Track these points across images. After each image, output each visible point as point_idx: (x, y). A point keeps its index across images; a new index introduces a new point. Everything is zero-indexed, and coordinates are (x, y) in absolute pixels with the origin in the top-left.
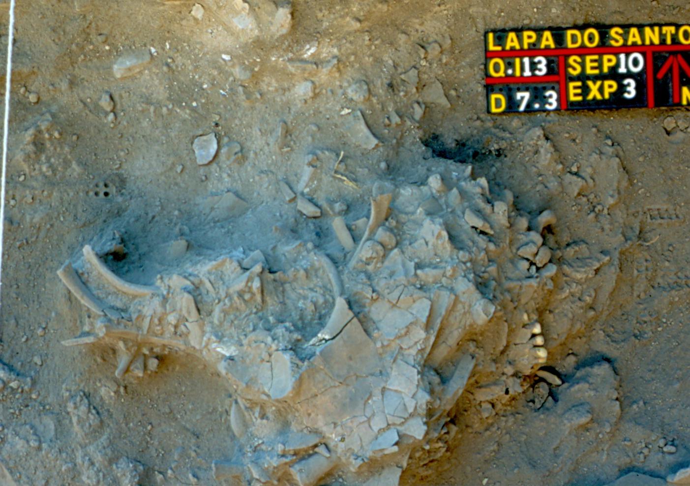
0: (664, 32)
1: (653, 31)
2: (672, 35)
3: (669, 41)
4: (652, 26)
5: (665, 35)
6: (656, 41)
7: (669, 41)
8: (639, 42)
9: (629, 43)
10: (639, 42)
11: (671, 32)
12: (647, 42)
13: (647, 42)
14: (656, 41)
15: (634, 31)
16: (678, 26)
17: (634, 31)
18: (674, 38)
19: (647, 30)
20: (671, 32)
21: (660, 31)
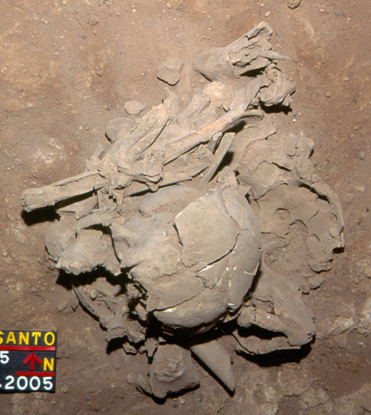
0: (33, 335)
1: (25, 335)
2: (38, 338)
3: (36, 343)
4: (25, 333)
5: (34, 338)
6: (27, 342)
7: (36, 343)
8: (15, 343)
9: (7, 342)
10: (15, 343)
11: (38, 335)
12: (20, 343)
13: (20, 343)
14: (27, 342)
15: (11, 334)
16: (43, 334)
17: (11, 334)
18: (41, 340)
19: (21, 335)
20: (38, 335)
21: (30, 335)
